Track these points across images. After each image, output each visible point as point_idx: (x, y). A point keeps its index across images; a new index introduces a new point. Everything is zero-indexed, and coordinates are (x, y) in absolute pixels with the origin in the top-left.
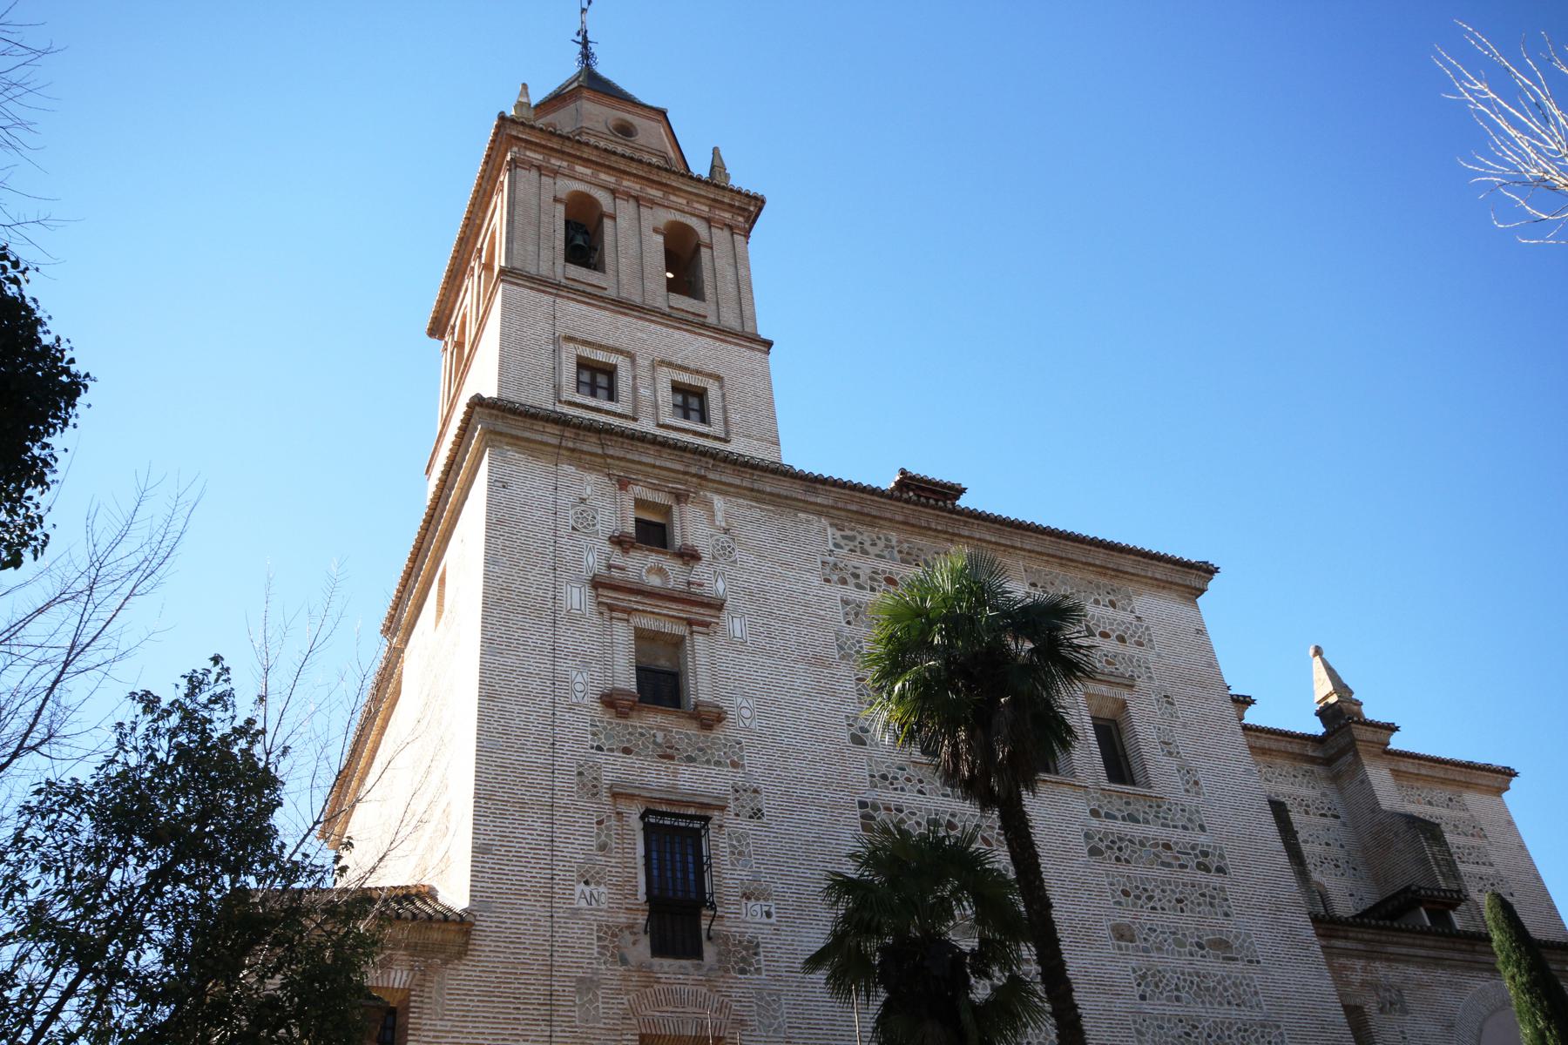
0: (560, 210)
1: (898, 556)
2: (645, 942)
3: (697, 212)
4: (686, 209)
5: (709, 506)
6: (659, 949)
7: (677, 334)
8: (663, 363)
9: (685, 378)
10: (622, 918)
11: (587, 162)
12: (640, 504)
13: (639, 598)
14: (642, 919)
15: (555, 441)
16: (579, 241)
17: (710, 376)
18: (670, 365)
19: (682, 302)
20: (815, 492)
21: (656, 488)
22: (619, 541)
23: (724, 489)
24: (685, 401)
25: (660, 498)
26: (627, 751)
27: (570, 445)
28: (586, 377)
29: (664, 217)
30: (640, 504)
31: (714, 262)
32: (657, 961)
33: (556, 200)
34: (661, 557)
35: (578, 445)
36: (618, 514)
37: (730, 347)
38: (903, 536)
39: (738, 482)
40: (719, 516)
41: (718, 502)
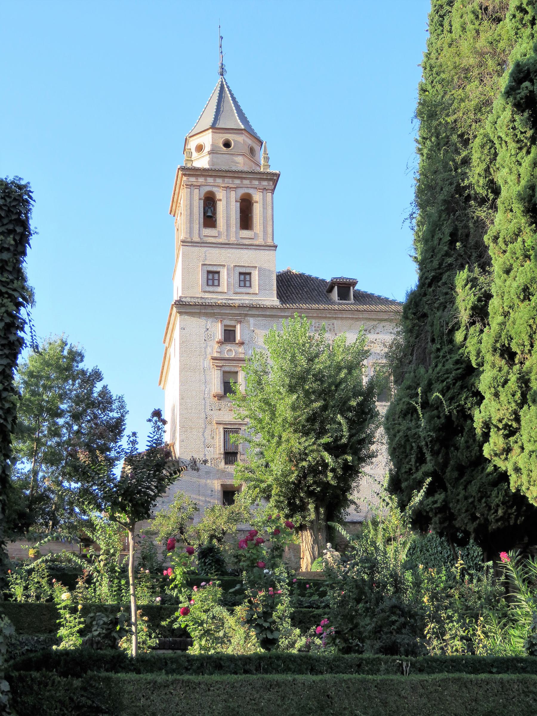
0: (202, 202)
1: (314, 329)
2: (223, 461)
3: (253, 186)
4: (249, 186)
5: (248, 322)
6: (226, 463)
7: (242, 251)
8: (235, 266)
9: (243, 270)
10: (217, 456)
11: (211, 176)
12: (225, 326)
13: (224, 362)
14: (222, 456)
15: (198, 311)
16: (209, 214)
17: (253, 267)
18: (239, 266)
19: (245, 233)
20: (285, 312)
21: (231, 320)
22: (220, 343)
23: (253, 316)
24: (245, 278)
25: (232, 323)
26: (220, 410)
27: (203, 311)
28: (210, 277)
29: (241, 192)
30: (225, 326)
31: (257, 210)
32: (226, 466)
33: (200, 199)
34: (232, 345)
35: (206, 311)
36: (218, 332)
37: (261, 251)
38: (317, 321)
39: (258, 313)
40: (252, 325)
41: (252, 320)
